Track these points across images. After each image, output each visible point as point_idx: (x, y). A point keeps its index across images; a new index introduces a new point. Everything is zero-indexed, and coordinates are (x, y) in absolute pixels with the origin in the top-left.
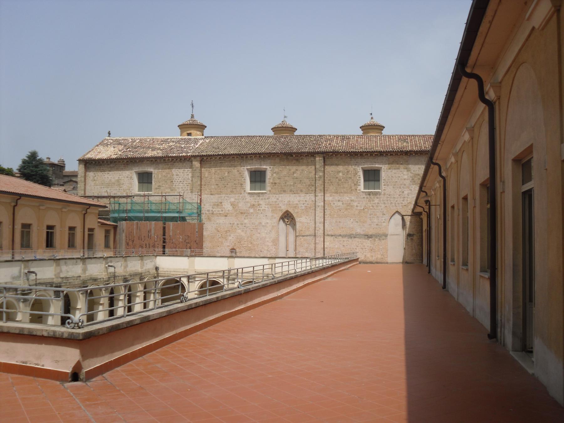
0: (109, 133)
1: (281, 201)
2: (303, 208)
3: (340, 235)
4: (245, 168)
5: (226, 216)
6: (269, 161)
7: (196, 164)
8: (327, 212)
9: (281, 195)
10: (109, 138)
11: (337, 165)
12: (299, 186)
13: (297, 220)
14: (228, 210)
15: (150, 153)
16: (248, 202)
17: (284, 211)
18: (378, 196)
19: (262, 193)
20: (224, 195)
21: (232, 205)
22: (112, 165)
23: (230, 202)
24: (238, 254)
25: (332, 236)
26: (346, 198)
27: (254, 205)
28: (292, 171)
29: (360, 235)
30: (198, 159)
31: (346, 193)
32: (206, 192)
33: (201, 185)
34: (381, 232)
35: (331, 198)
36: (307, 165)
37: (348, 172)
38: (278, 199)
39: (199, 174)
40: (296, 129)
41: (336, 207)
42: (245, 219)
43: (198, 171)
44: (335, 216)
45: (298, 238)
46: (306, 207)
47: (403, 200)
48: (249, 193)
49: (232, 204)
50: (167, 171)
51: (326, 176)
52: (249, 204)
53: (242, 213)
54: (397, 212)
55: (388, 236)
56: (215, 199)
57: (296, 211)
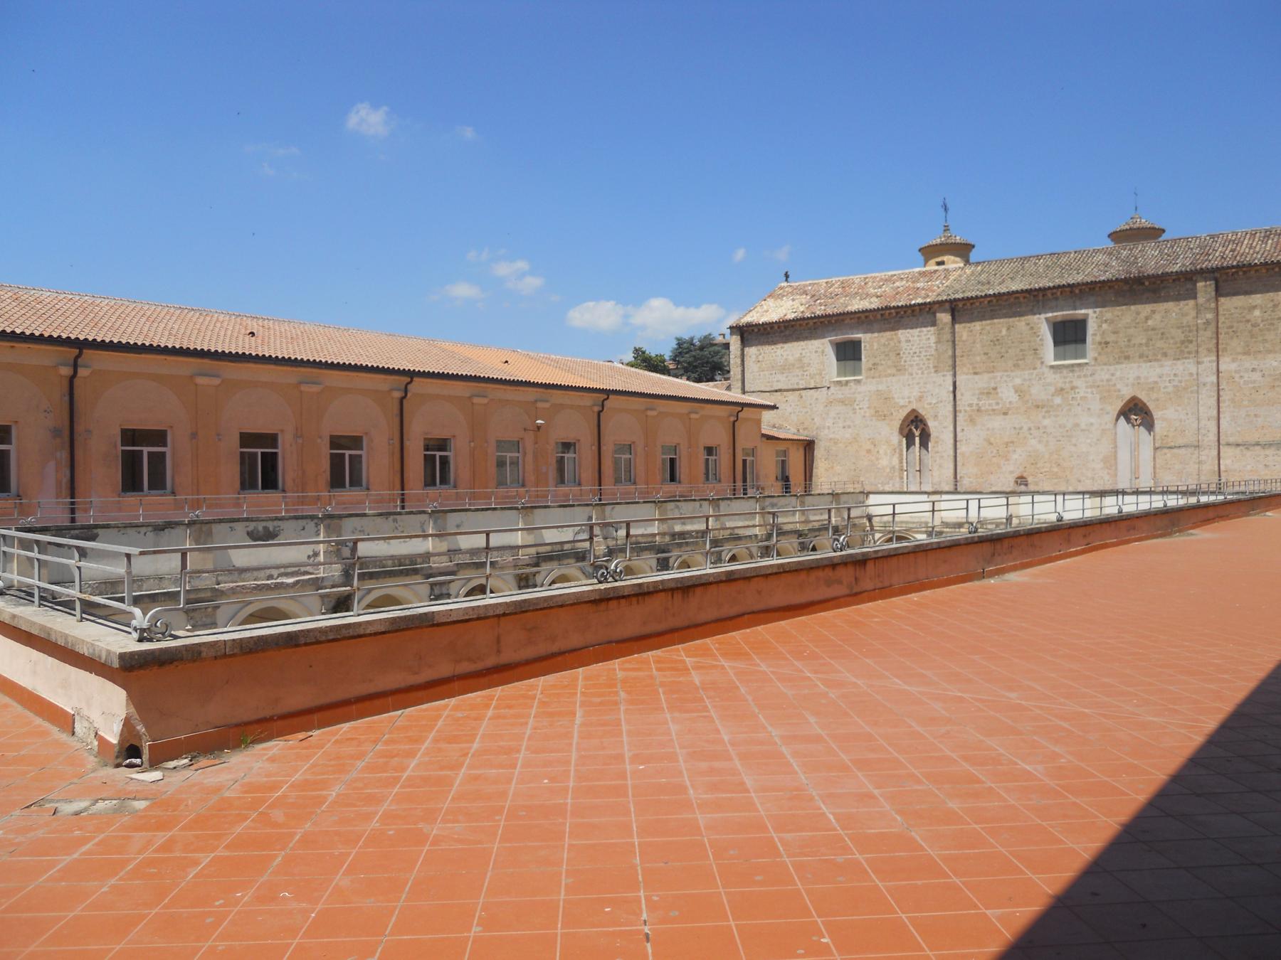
0: (787, 276)
1: (1121, 379)
2: (1170, 389)
3: (1258, 444)
4: (1043, 316)
5: (1005, 414)
6: (1092, 299)
7: (944, 318)
8: (1225, 396)
9: (1118, 366)
10: (785, 284)
11: (1247, 293)
12: (1159, 344)
13: (1157, 414)
15: (856, 305)
16: (1050, 384)
17: (1128, 398)
19: (1079, 365)
20: (999, 374)
22: (787, 333)
24: (1032, 488)
25: (1238, 445)
27: (1062, 389)
28: (1143, 315)
30: (947, 306)
31: (1269, 352)
32: (965, 370)
33: (954, 356)
35: (1233, 366)
36: (1178, 298)
39: (949, 336)
40: (1164, 231)
43: (948, 329)
44: (1246, 403)
46: (1175, 386)
48: (1052, 367)
49: (1019, 391)
50: (888, 334)
51: (1222, 319)
52: (1052, 389)
56: (983, 381)
57: (1154, 396)
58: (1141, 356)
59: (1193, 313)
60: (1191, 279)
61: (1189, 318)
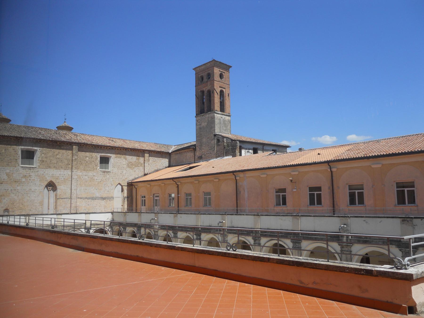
2: (63, 179)
3: (86, 198)
4: (20, 147)
12: (60, 164)
13: (58, 187)
14: (4, 179)
18: (109, 174)
19: (33, 167)
21: (7, 175)
23: (6, 173)
24: (11, 213)
26: (91, 174)
27: (25, 176)
29: (98, 197)
31: (90, 170)
34: (110, 196)
36: (67, 149)
37: (92, 157)
38: (45, 172)
40: (11, 121)
41: (84, 179)
42: (18, 186)
45: (58, 201)
46: (64, 178)
48: (22, 167)
49: (7, 175)
52: (22, 175)
53: (16, 182)
54: (119, 184)
57: (58, 181)
58: (54, 167)
59: (71, 155)
60: (71, 145)
61: (70, 157)
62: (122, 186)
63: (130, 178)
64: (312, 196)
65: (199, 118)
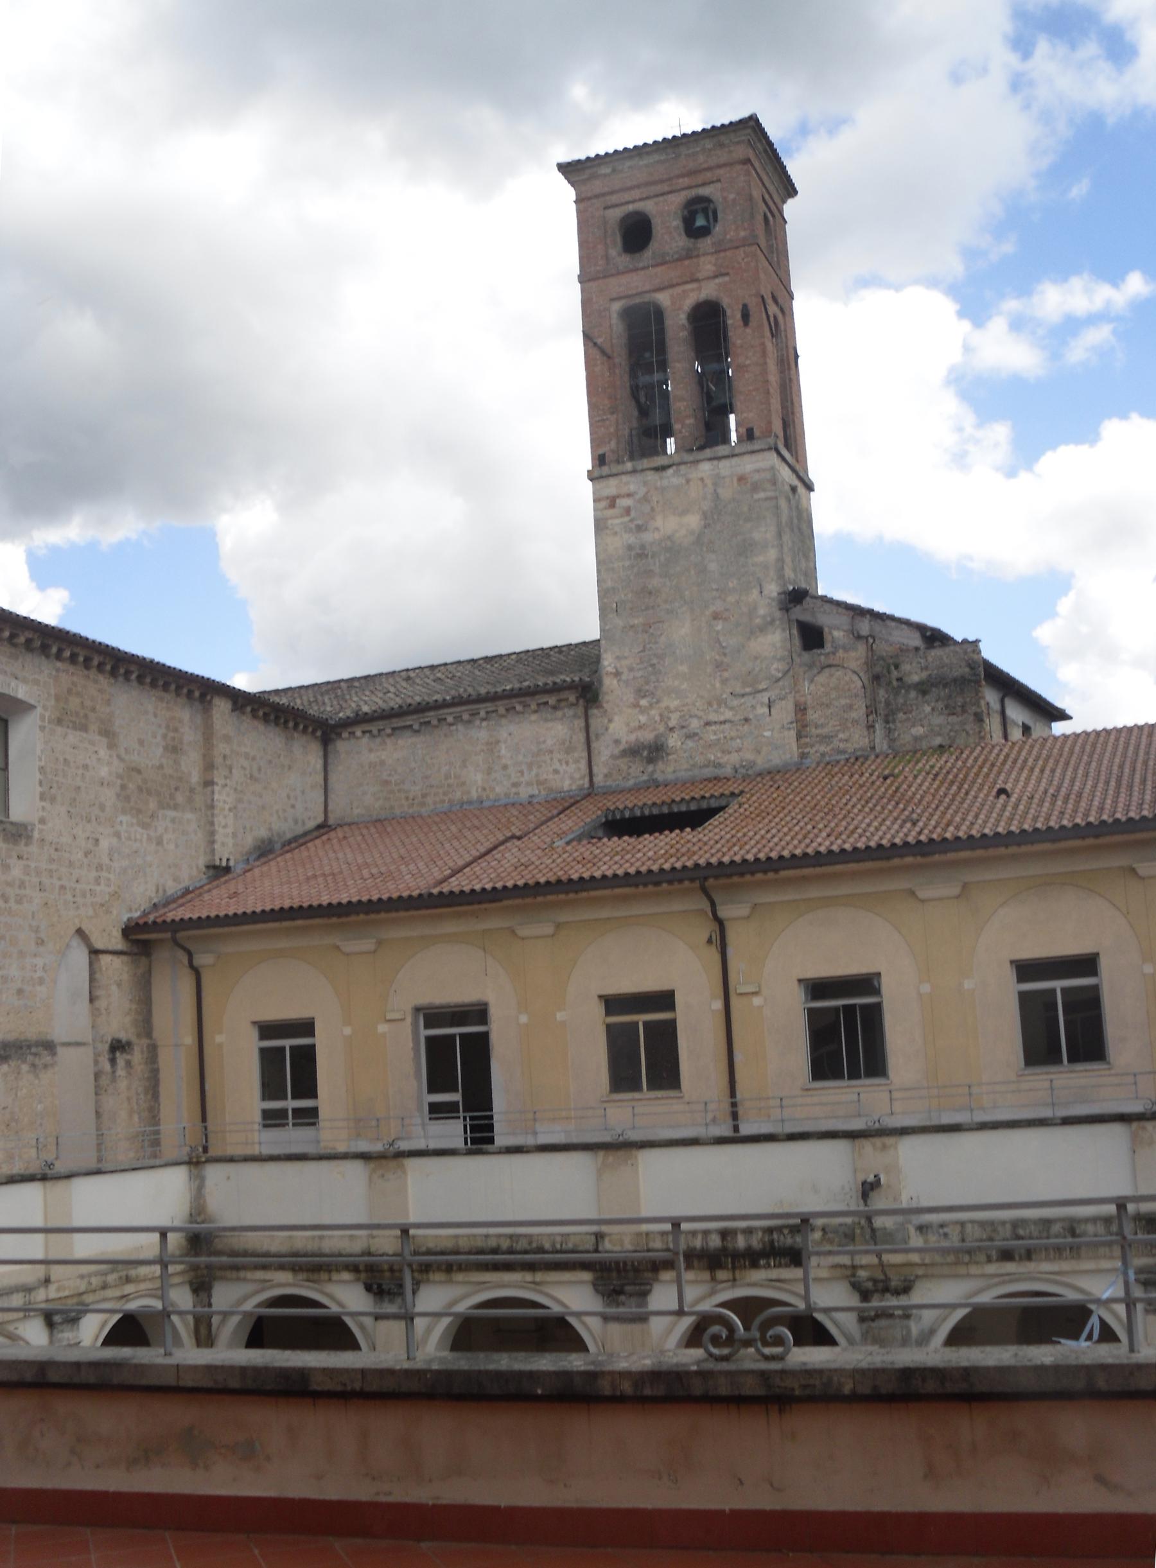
18: (22, 848)
34: (31, 1034)
47: (97, 880)
55: (59, 1050)
62: (94, 952)
63: (139, 898)
64: (1035, 1011)
65: (612, 487)
